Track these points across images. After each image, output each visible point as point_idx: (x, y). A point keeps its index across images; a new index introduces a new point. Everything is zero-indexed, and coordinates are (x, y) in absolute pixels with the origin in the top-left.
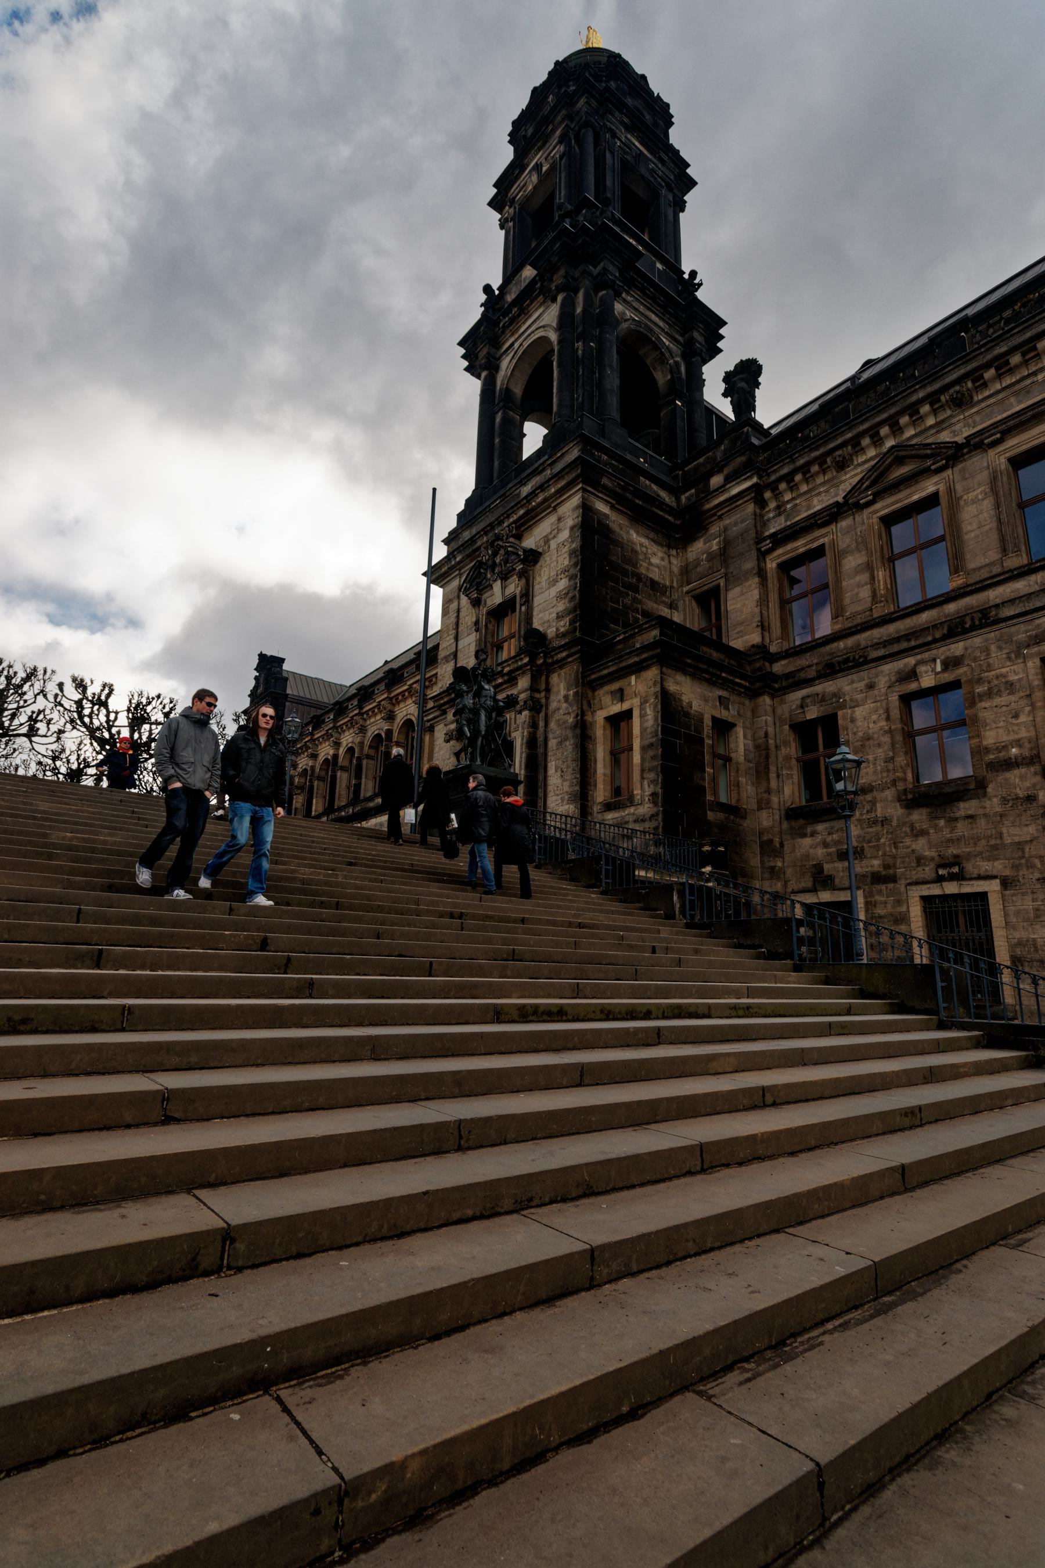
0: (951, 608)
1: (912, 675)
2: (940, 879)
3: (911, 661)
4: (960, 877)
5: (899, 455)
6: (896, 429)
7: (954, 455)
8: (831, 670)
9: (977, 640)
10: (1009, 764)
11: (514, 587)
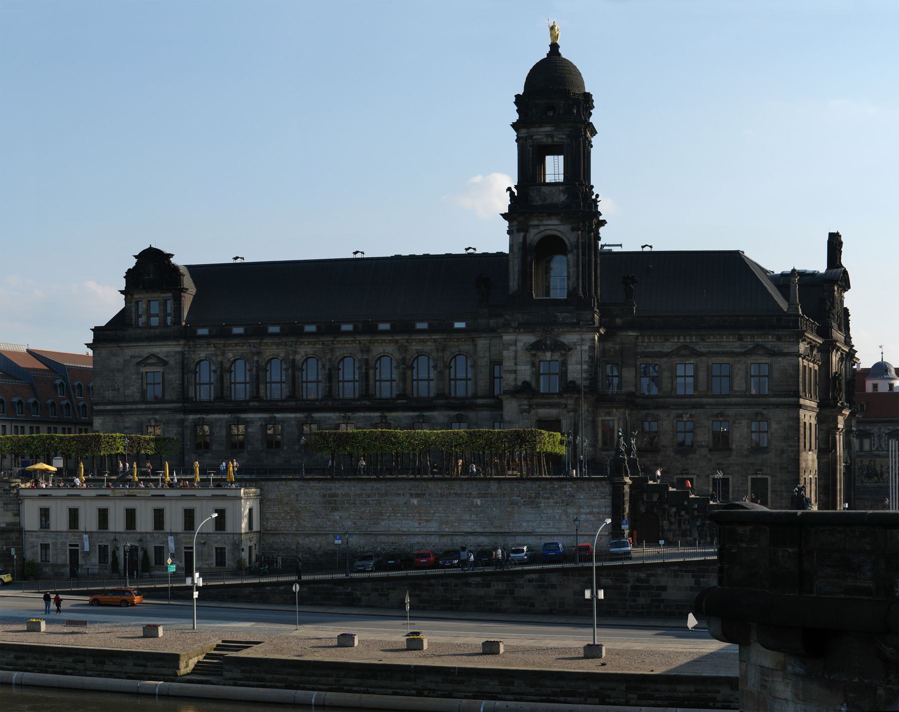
0: (693, 400)
1: (681, 416)
2: (682, 474)
3: (681, 412)
4: (687, 474)
5: (685, 347)
6: (685, 338)
7: (699, 354)
8: (657, 407)
9: (699, 411)
10: (702, 446)
11: (557, 356)
